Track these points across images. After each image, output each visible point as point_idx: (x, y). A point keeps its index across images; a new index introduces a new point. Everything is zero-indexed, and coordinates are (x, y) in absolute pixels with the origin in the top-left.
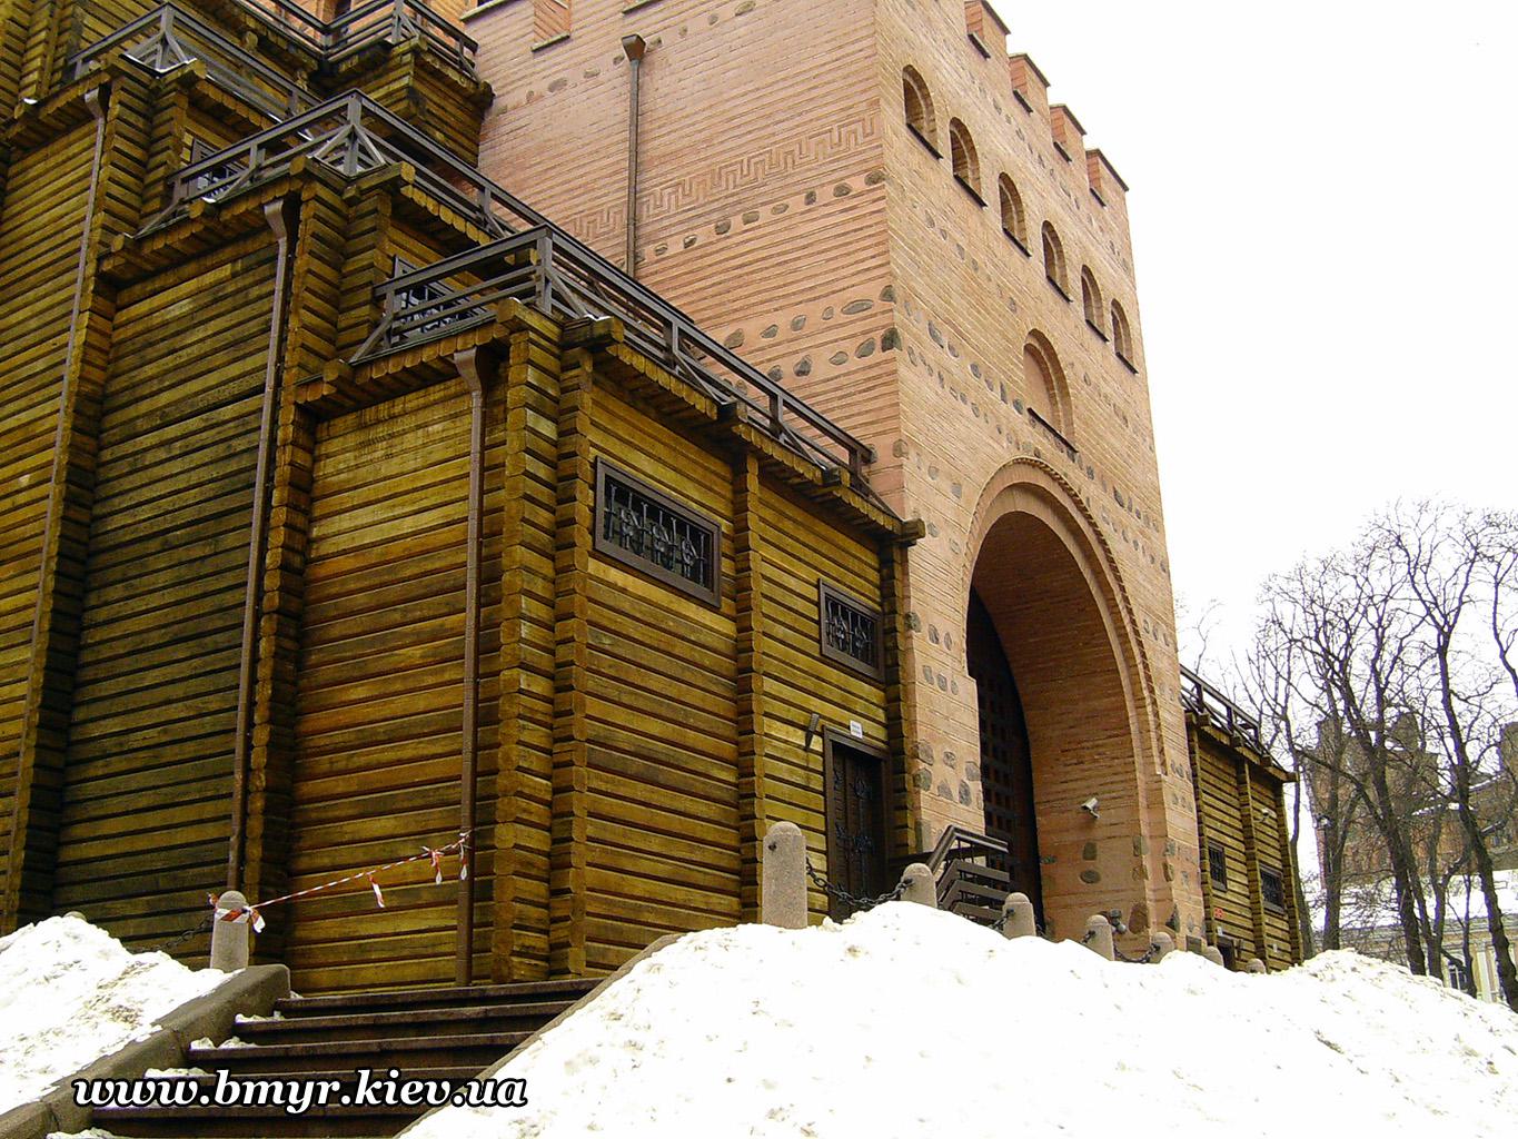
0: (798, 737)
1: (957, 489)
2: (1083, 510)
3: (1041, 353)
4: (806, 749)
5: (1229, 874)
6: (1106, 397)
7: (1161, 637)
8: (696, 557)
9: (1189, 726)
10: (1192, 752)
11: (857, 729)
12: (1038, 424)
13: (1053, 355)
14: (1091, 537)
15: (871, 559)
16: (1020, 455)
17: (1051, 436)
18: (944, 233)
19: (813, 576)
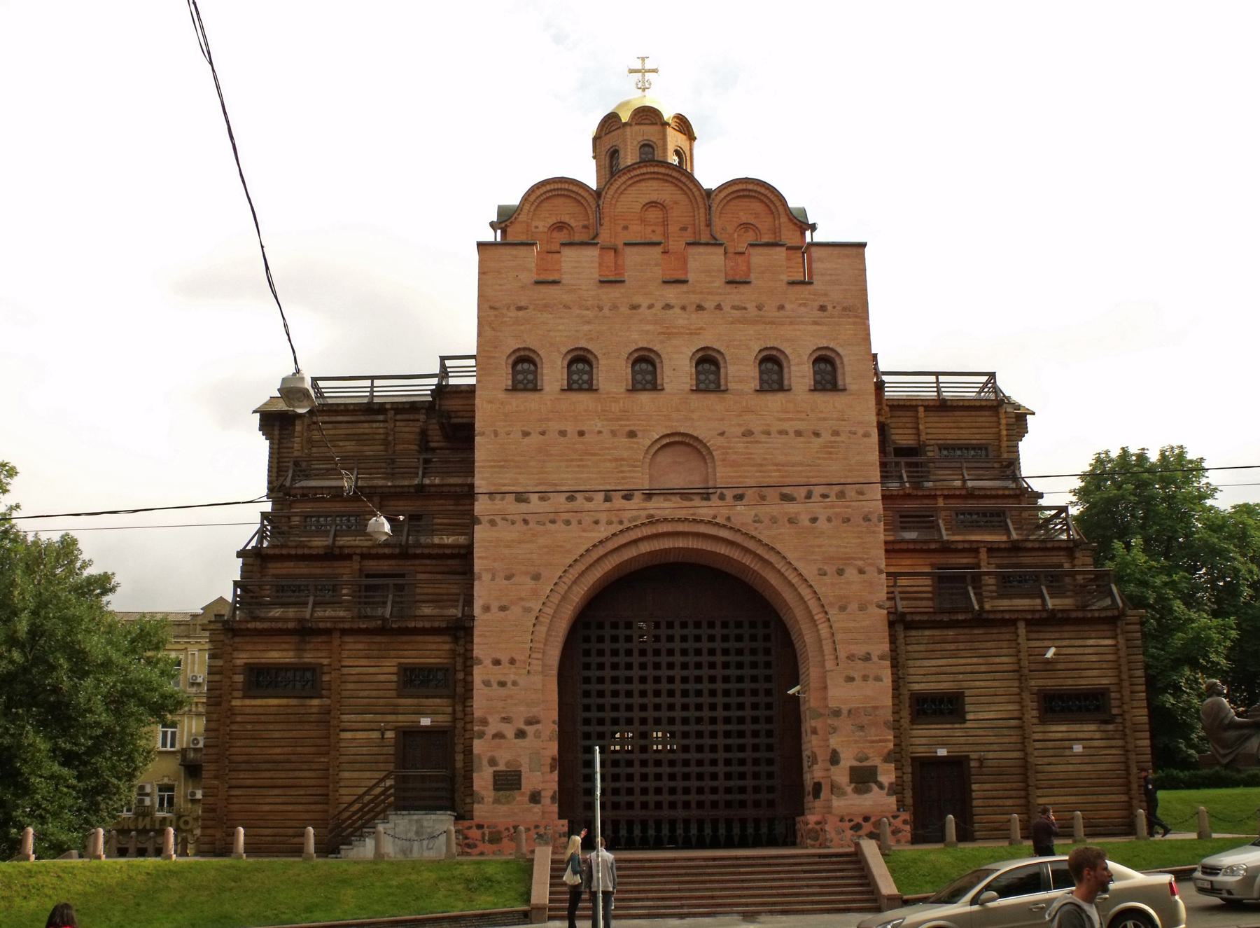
0: (376, 735)
1: (536, 577)
2: (724, 526)
3: (683, 443)
4: (383, 738)
5: (967, 708)
6: (783, 432)
7: (851, 573)
8: (305, 680)
9: (891, 624)
10: (893, 640)
11: (425, 721)
12: (655, 499)
13: (696, 439)
14: (738, 538)
15: (447, 639)
16: (621, 527)
17: (678, 498)
18: (543, 433)
19: (395, 662)
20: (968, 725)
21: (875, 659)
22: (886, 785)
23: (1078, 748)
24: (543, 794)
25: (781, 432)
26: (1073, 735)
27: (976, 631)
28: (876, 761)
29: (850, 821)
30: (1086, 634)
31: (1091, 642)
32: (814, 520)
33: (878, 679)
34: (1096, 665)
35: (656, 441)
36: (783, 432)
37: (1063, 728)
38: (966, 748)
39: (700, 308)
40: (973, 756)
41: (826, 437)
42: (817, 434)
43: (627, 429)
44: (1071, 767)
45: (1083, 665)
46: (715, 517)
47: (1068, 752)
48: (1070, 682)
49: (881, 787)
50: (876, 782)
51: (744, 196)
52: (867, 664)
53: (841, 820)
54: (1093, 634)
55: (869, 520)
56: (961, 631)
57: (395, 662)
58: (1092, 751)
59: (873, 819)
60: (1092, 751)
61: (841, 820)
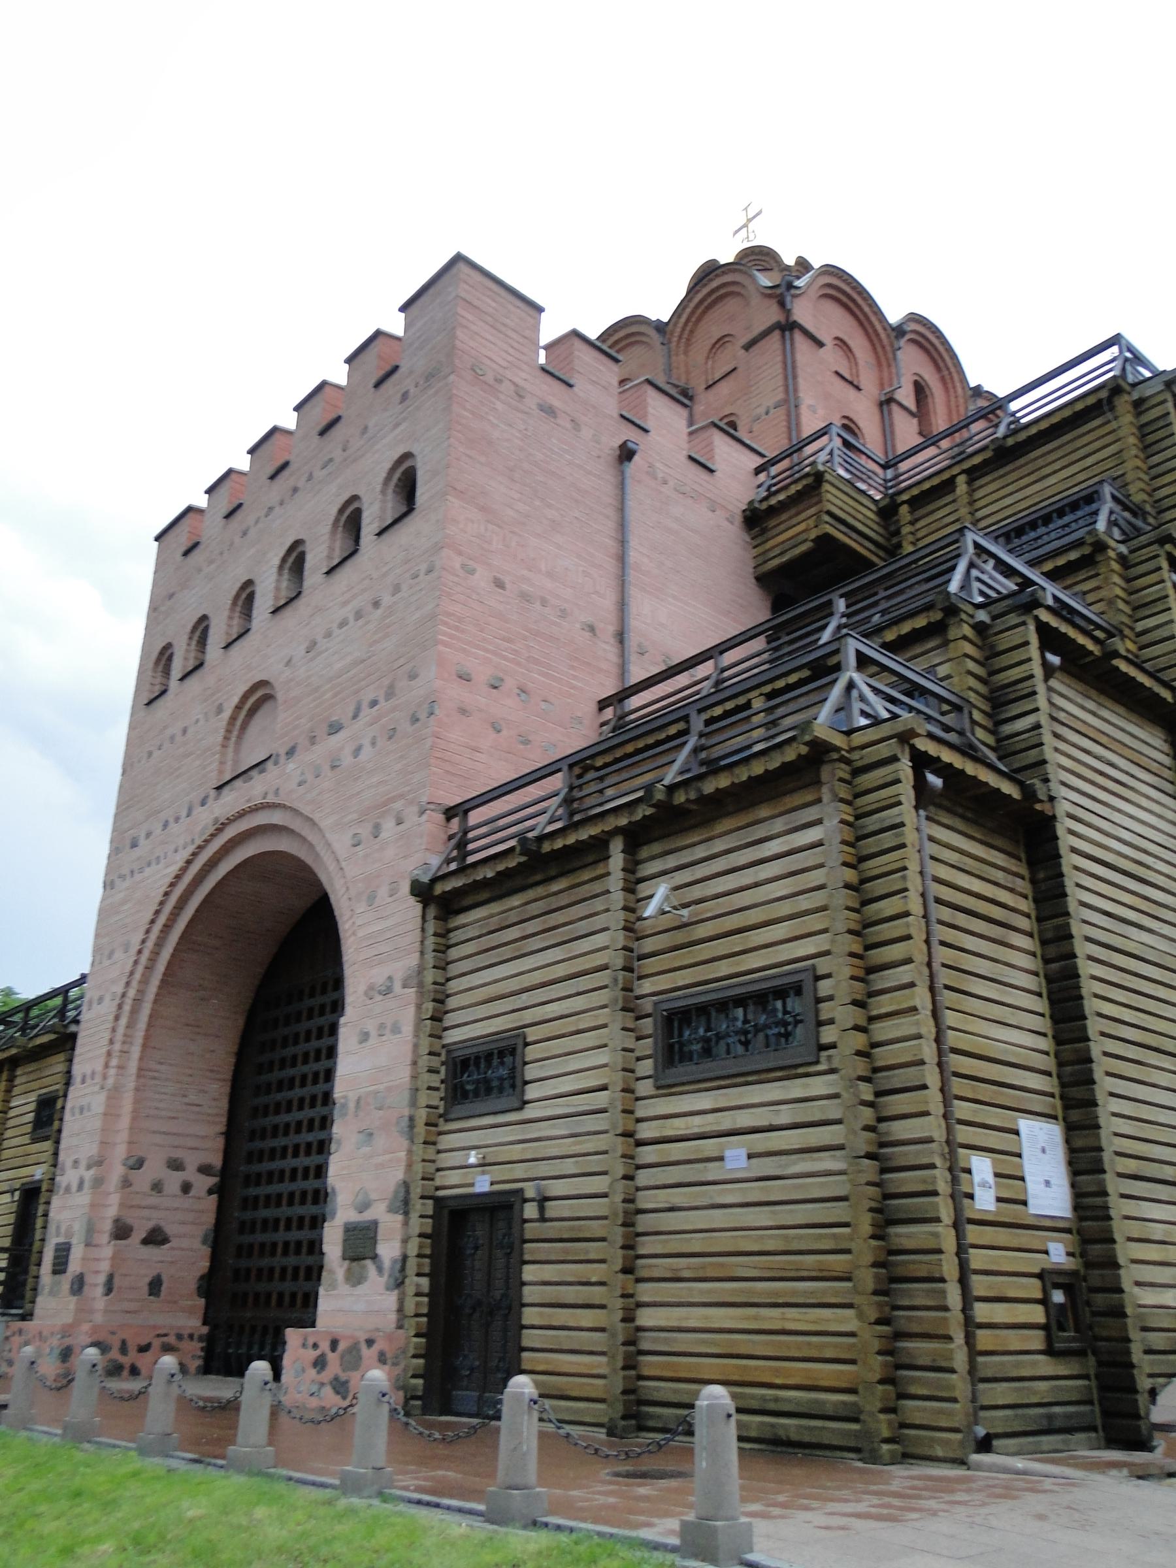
5: (531, 1072)
20: (530, 1112)
21: (397, 987)
22: (387, 1264)
23: (736, 1156)
24: (88, 1279)
25: (343, 624)
26: (726, 1121)
27: (555, 887)
29: (315, 1346)
30: (760, 832)
31: (774, 847)
33: (396, 1030)
34: (786, 908)
35: (238, 708)
36: (343, 624)
37: (705, 1101)
38: (519, 1171)
39: (295, 490)
40: (530, 1191)
41: (387, 600)
42: (376, 604)
43: (217, 703)
44: (718, 1218)
46: (265, 796)
47: (712, 1172)
48: (724, 968)
49: (380, 1269)
50: (375, 1257)
51: (715, 302)
53: (304, 1346)
54: (779, 825)
55: (418, 720)
56: (531, 894)
57: (33, 1097)
58: (768, 1166)
59: (342, 1346)
60: (768, 1166)
61: (304, 1346)
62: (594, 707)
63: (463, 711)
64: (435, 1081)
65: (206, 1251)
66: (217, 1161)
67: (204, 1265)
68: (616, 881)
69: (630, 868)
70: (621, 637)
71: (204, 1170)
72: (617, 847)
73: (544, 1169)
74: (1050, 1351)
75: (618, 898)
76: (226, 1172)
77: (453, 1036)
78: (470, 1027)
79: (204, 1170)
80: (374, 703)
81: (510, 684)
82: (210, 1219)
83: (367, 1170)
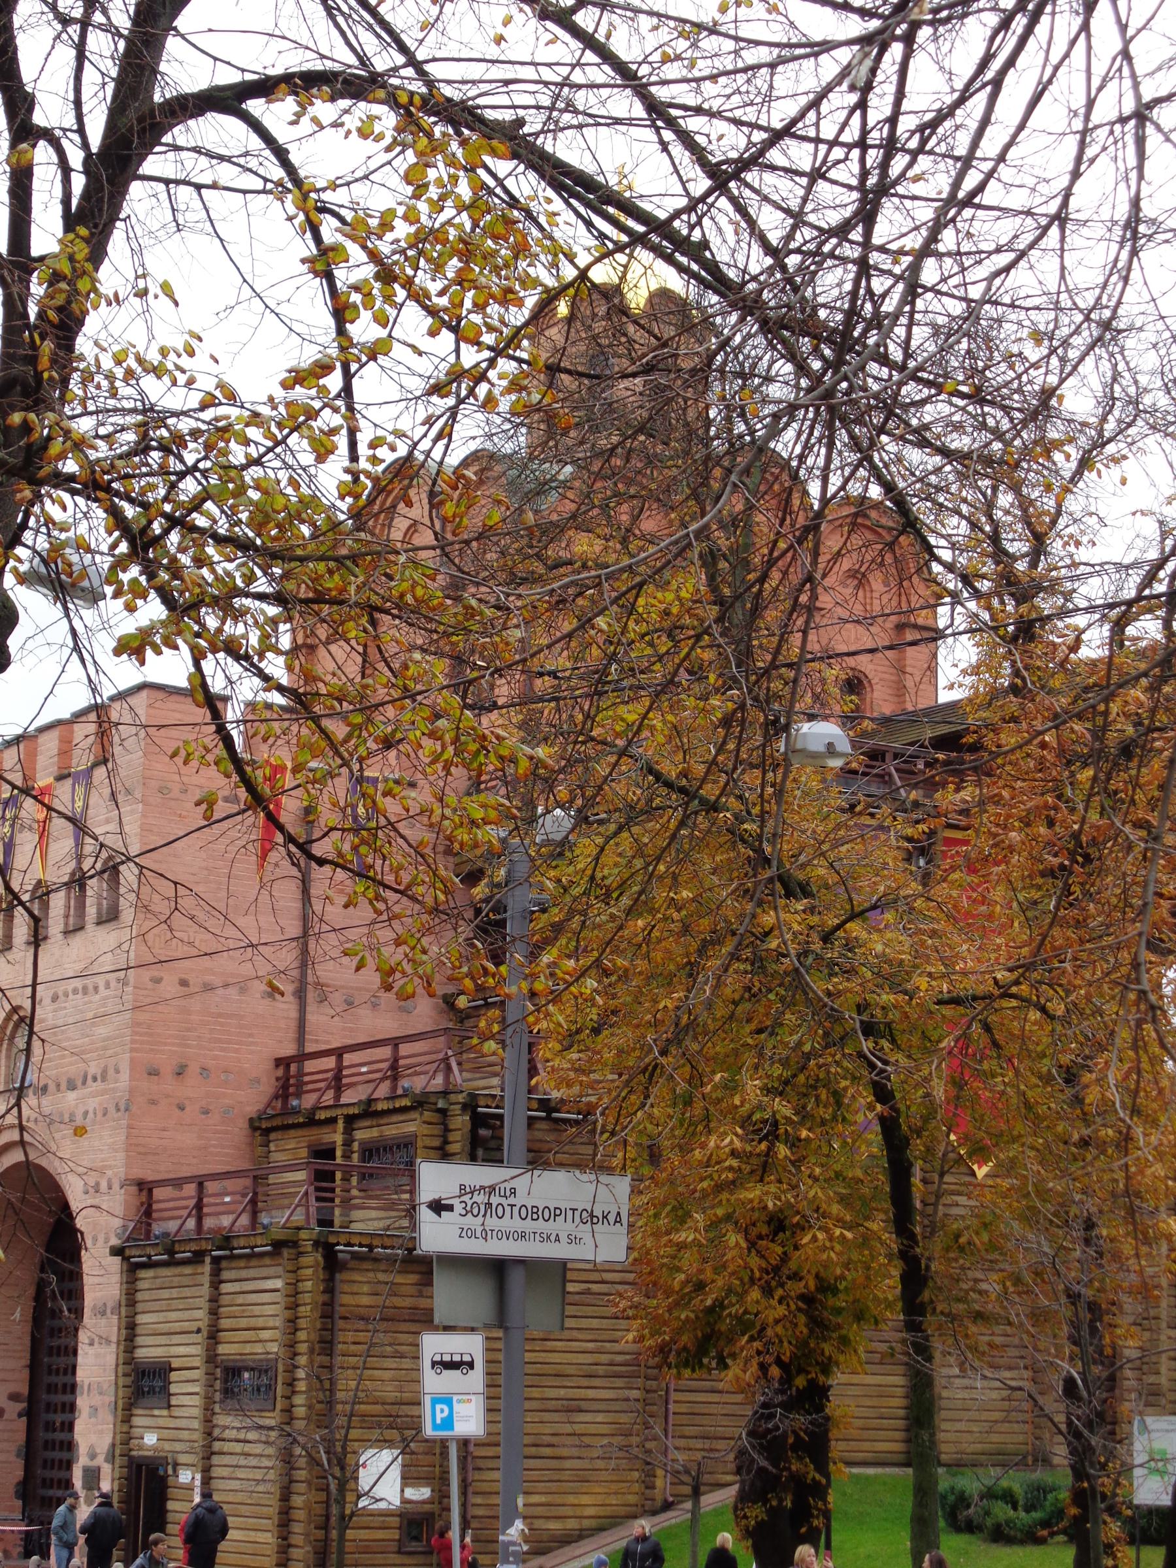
5: (173, 1389)
28: (100, 1461)
32: (86, 1113)
33: (108, 1342)
45: (260, 1322)
48: (248, 1349)
52: (103, 1321)
62: (272, 1064)
63: (153, 1102)
64: (128, 1381)
65: (21, 1463)
66: (25, 1390)
67: (20, 1474)
68: (206, 1279)
69: (216, 1272)
70: (300, 994)
71: (14, 1397)
72: (208, 1260)
73: (178, 1446)
74: (399, 1552)
75: (205, 1290)
76: (32, 1399)
77: (140, 1353)
78: (149, 1351)
79: (14, 1397)
80: (95, 1079)
81: (194, 1068)
82: (21, 1437)
83: (93, 1434)
